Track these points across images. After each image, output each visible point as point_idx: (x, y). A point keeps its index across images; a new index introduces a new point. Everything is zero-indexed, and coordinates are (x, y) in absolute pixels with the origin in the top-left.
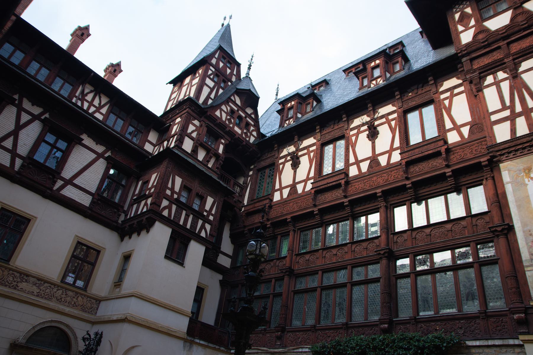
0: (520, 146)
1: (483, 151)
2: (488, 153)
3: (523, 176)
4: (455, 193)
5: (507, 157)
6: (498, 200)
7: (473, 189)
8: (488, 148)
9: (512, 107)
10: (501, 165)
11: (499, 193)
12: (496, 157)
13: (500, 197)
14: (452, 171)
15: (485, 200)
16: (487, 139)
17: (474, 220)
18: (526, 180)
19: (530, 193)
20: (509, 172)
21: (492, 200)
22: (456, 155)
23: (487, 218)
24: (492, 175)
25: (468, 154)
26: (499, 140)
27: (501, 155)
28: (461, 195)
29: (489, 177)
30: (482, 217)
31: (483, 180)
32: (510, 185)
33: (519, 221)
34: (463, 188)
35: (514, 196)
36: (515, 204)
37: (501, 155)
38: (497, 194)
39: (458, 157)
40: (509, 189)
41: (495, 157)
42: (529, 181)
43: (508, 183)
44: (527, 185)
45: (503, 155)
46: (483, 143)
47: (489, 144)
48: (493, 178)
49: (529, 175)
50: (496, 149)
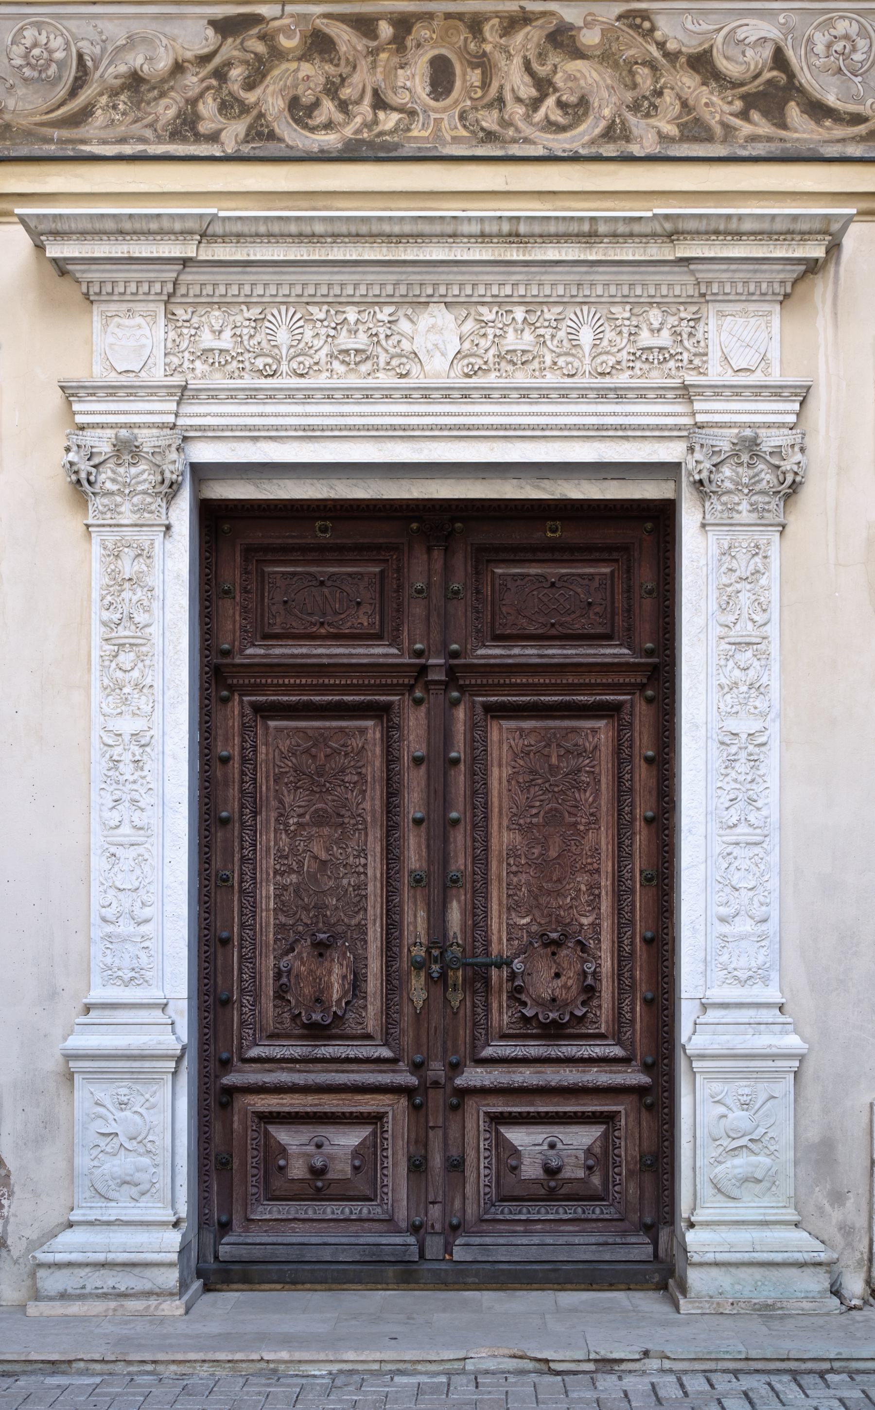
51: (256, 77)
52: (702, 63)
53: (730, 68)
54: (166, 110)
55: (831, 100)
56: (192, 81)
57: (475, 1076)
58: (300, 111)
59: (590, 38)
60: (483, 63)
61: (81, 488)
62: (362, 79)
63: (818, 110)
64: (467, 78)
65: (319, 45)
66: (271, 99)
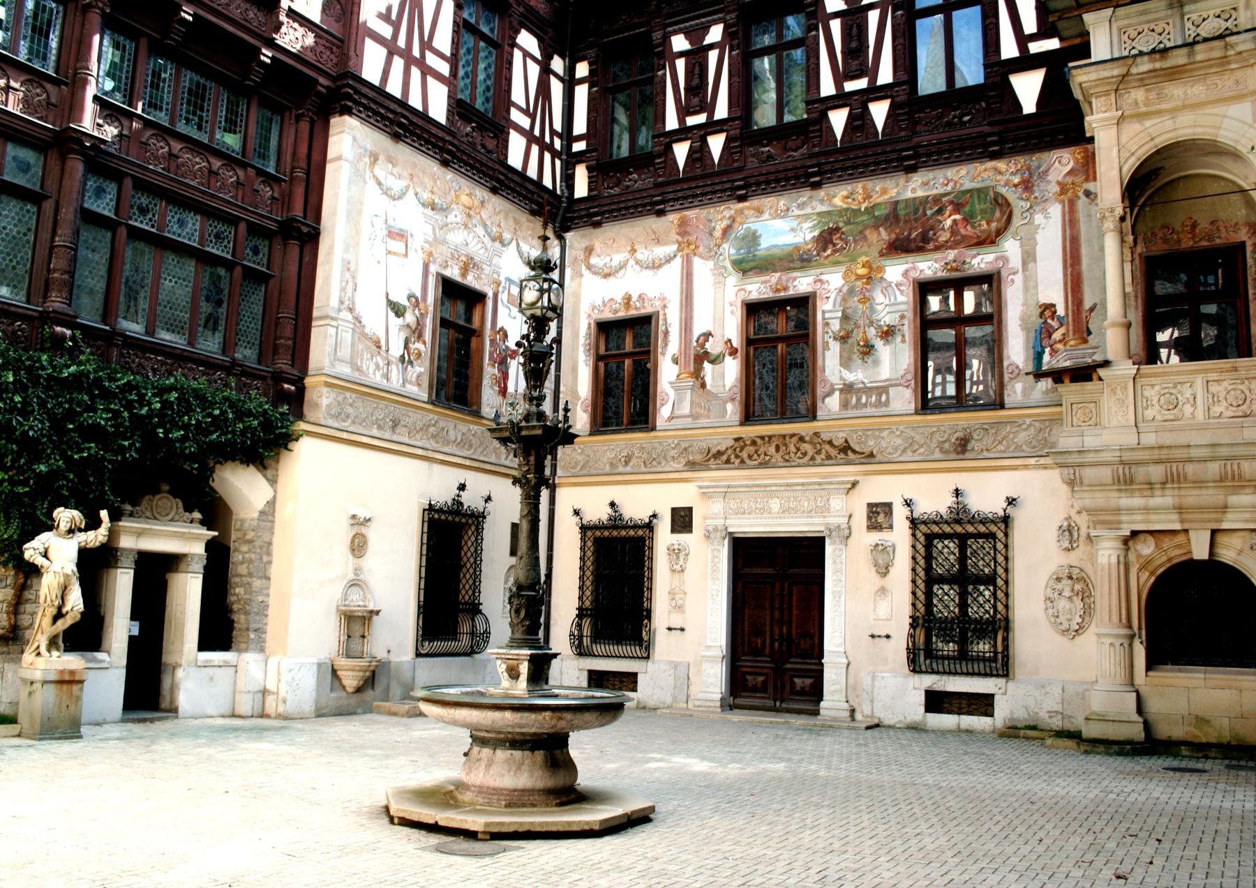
9: (396, 26)
51: (742, 450)
52: (830, 443)
53: (836, 443)
54: (724, 458)
55: (857, 449)
56: (729, 452)
57: (789, 666)
58: (750, 457)
59: (807, 439)
60: (786, 445)
61: (708, 537)
62: (762, 450)
63: (854, 452)
64: (783, 448)
65: (754, 443)
66: (744, 455)
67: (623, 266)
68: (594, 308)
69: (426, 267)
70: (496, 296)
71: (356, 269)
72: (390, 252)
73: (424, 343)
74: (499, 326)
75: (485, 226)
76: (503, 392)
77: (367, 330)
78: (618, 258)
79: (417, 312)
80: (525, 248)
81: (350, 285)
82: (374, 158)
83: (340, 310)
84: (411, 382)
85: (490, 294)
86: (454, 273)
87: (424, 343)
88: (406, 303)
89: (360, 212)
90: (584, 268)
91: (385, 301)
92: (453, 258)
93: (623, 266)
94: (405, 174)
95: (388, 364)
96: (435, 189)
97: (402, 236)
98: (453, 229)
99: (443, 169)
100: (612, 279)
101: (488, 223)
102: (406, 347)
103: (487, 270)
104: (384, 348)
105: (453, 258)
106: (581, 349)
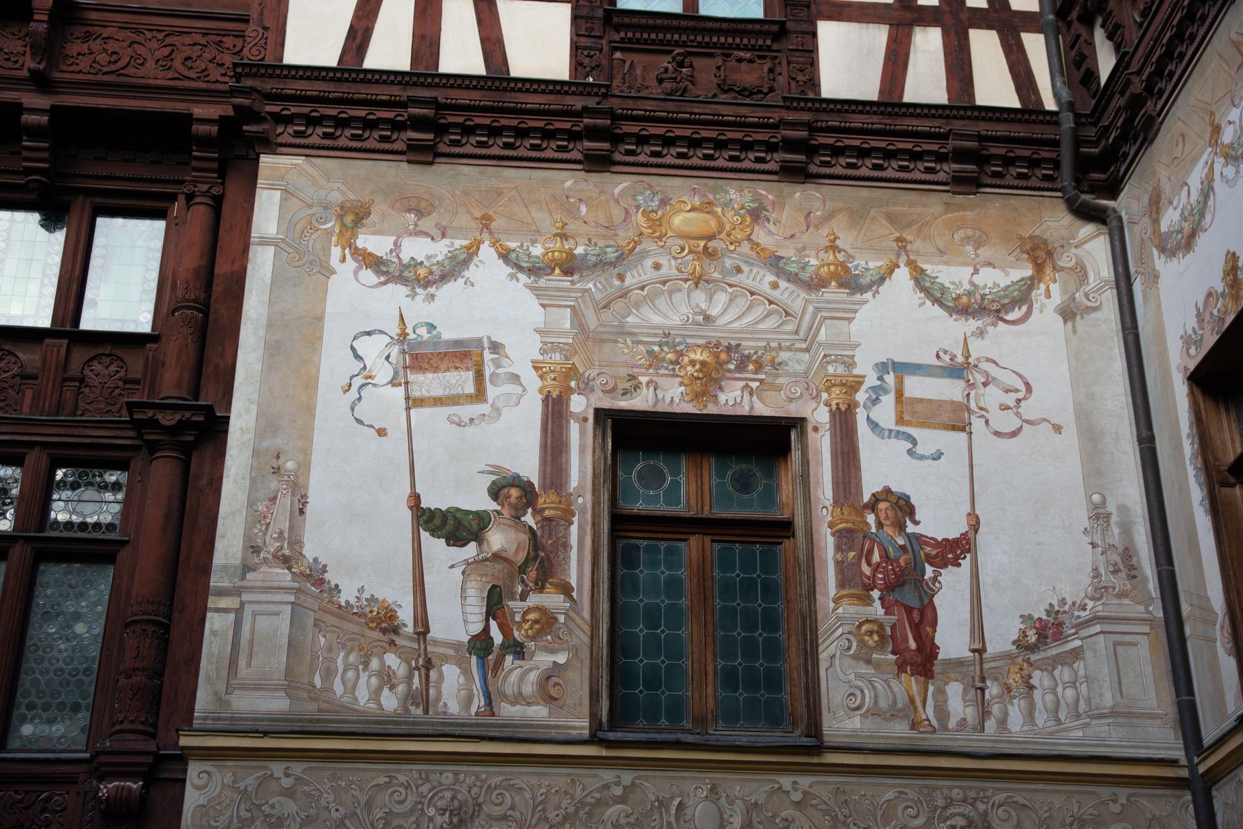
0: (361, 112)
1: (215, 73)
2: (233, 92)
3: (329, 233)
4: (35, 217)
5: (298, 134)
6: (203, 301)
7: (119, 221)
8: (243, 70)
10: (265, 160)
11: (217, 271)
12: (256, 117)
13: (218, 287)
14: (55, 111)
15: (154, 285)
16: (251, 30)
17: (80, 355)
18: (336, 252)
19: (329, 309)
20: (283, 200)
21: (180, 293)
22: (96, 45)
23: (135, 363)
24: (216, 191)
25: (151, 64)
26: (294, 54)
27: (279, 119)
28: (60, 236)
29: (204, 194)
30: (119, 352)
31: (173, 198)
32: (271, 250)
33: (254, 408)
34: (81, 206)
35: (271, 303)
36: (262, 332)
37: (279, 119)
38: (207, 275)
39: (103, 58)
40: (262, 266)
41: (256, 117)
42: (343, 260)
43: (265, 242)
44: (333, 272)
45: (288, 120)
46: (229, 41)
47: (251, 54)
48: (217, 205)
49: (354, 236)
50: (269, 86)
67: (1207, 191)
68: (1188, 341)
69: (555, 412)
70: (844, 422)
71: (305, 467)
72: (420, 402)
73: (566, 589)
74: (870, 485)
75: (775, 263)
76: (922, 661)
77: (348, 595)
78: (1195, 180)
79: (529, 519)
80: (953, 276)
81: (286, 502)
82: (355, 217)
83: (246, 568)
84: (518, 699)
85: (820, 416)
86: (669, 395)
87: (566, 589)
88: (490, 505)
89: (314, 340)
90: (1155, 252)
91: (406, 516)
92: (655, 360)
93: (1207, 191)
94: (464, 220)
95: (428, 665)
96: (572, 227)
97: (465, 355)
98: (651, 299)
99: (595, 177)
100: (1202, 241)
101: (788, 252)
102: (495, 604)
103: (796, 362)
104: (410, 629)
105: (655, 360)
106: (1191, 472)
